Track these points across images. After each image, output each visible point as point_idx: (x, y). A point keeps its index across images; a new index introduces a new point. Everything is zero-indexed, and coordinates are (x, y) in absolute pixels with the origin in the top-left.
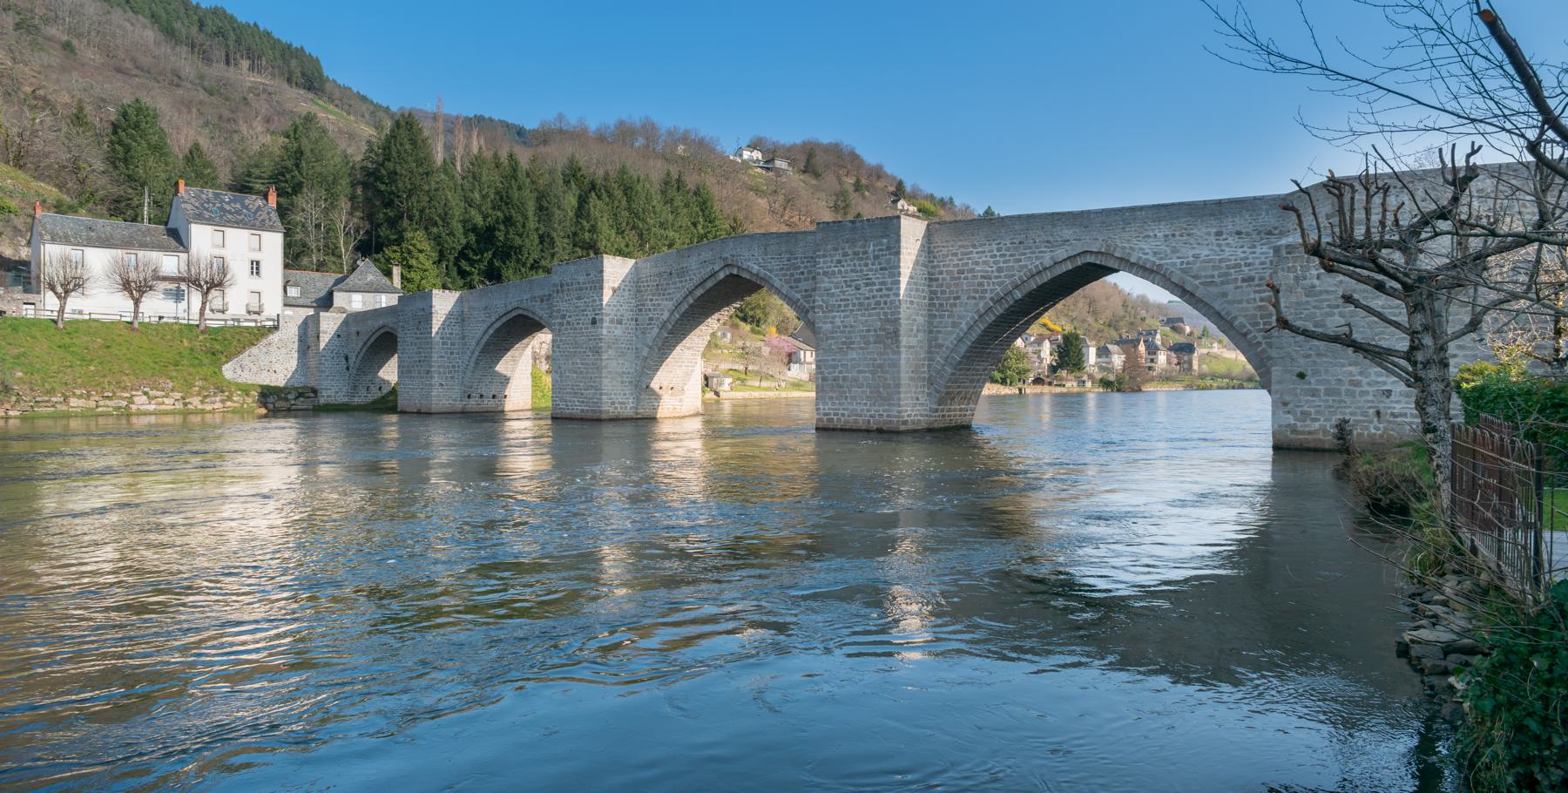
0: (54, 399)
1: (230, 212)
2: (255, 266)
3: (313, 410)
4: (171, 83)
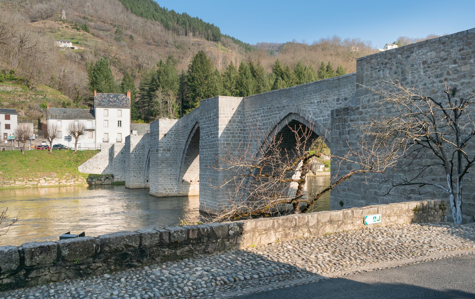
0: (11, 182)
1: (112, 102)
2: (120, 123)
3: (111, 184)
4: (165, 46)
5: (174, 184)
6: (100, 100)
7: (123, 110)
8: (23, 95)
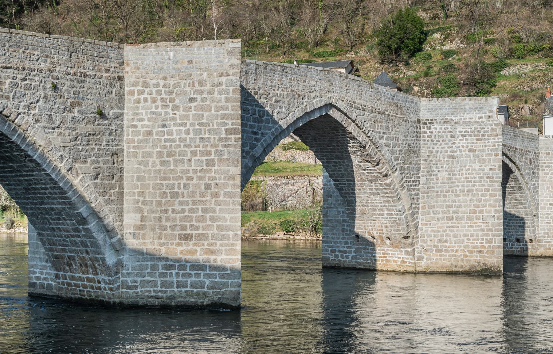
5: (349, 241)
8: (539, 76)
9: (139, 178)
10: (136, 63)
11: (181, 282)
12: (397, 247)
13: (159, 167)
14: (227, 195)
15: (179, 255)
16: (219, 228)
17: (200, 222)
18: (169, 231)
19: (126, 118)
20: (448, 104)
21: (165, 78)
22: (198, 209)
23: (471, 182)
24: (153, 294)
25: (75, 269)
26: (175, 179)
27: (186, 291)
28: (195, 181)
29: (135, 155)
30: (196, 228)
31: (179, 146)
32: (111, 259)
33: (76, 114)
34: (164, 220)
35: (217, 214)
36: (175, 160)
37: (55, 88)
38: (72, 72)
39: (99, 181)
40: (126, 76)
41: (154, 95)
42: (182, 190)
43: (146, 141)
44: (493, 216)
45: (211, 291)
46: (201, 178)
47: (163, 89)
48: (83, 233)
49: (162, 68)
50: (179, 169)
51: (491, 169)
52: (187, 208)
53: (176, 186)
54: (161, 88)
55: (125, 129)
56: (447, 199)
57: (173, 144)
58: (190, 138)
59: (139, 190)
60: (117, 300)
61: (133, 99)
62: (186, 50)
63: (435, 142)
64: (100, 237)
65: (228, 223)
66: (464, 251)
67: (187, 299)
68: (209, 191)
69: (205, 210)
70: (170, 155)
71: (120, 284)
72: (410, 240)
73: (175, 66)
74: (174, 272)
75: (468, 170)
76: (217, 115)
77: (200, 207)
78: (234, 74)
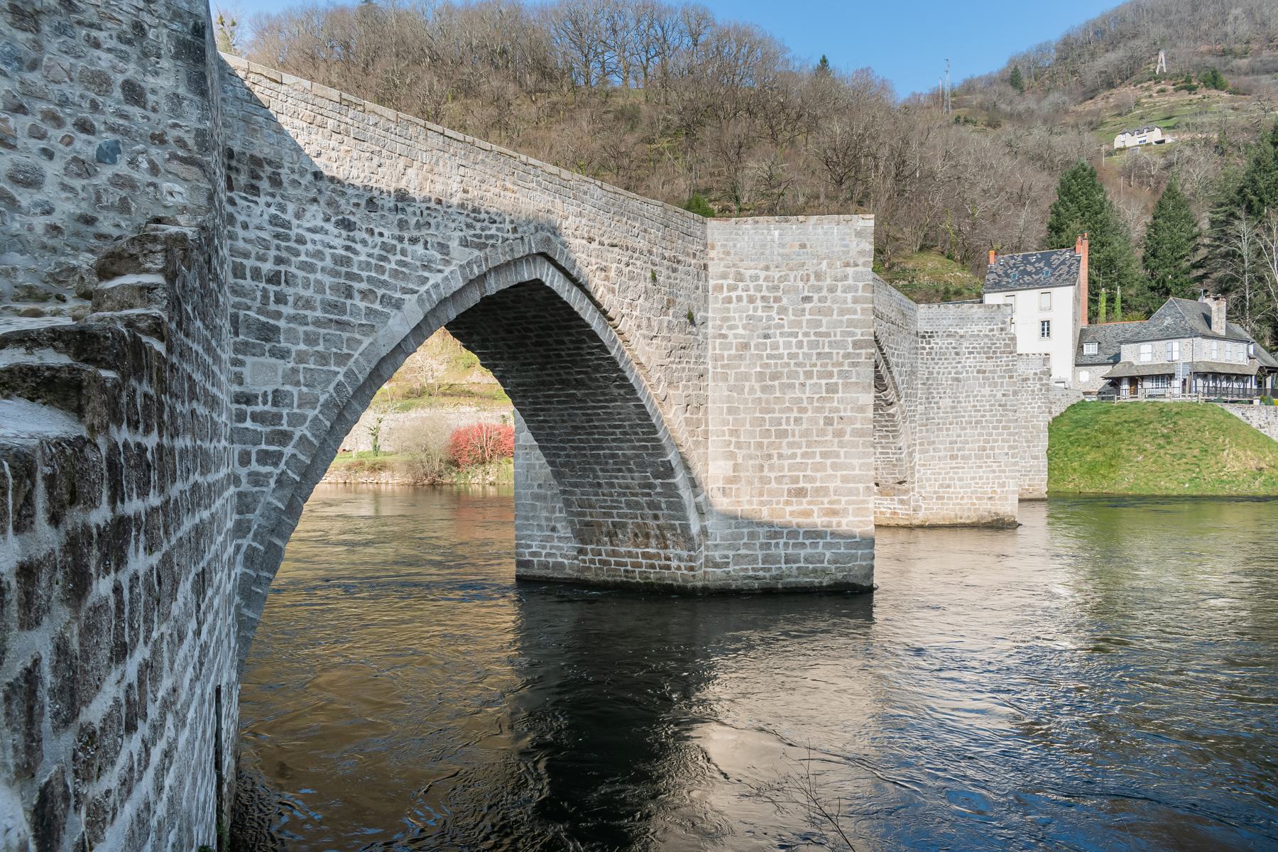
1: (1030, 274)
6: (1001, 272)
7: (1056, 291)
9: (731, 411)
10: (725, 246)
11: (790, 555)
12: (887, 495)
13: (759, 394)
14: (856, 433)
15: (788, 518)
16: (845, 480)
17: (817, 471)
18: (774, 485)
19: (710, 324)
20: (951, 312)
21: (767, 268)
22: (814, 453)
23: (980, 411)
24: (751, 573)
25: (621, 541)
26: (781, 411)
27: (798, 568)
28: (810, 414)
29: (725, 378)
30: (812, 480)
31: (788, 365)
32: (695, 529)
33: (671, 318)
34: (766, 470)
35: (842, 460)
36: (782, 386)
37: (654, 279)
38: (667, 255)
39: (688, 415)
40: (710, 263)
41: (752, 292)
42: (792, 426)
43: (741, 357)
44: (1007, 454)
45: (833, 567)
46: (818, 410)
47: (765, 284)
48: (659, 490)
49: (763, 254)
50: (787, 397)
51: (1004, 395)
52: (799, 452)
53: (784, 421)
54: (761, 282)
55: (709, 341)
56: (951, 433)
57: (779, 362)
58: (803, 353)
59: (731, 427)
60: (699, 584)
61: (720, 297)
62: (798, 229)
63: (936, 361)
64: (686, 494)
65: (857, 472)
66: (971, 498)
67: (798, 580)
68: (830, 428)
69: (824, 455)
70: (774, 377)
71: (702, 560)
72: (905, 486)
73: (781, 251)
74: (782, 541)
75: (976, 396)
76: (842, 321)
77: (818, 450)
78: (864, 264)
